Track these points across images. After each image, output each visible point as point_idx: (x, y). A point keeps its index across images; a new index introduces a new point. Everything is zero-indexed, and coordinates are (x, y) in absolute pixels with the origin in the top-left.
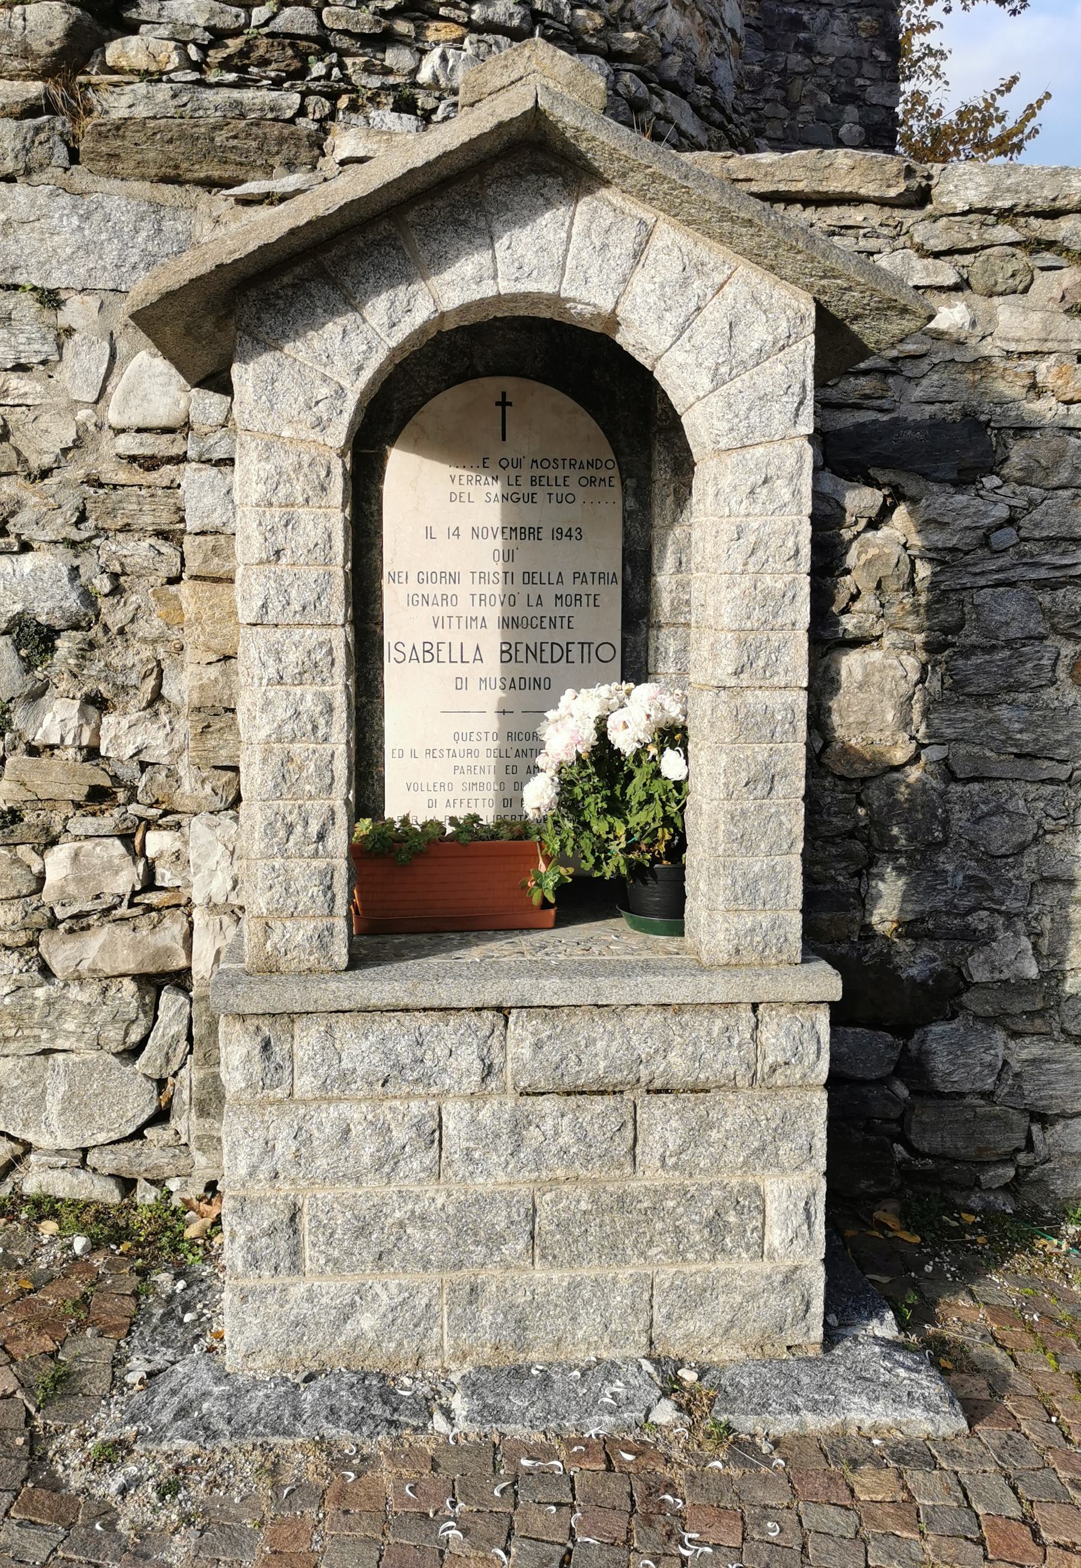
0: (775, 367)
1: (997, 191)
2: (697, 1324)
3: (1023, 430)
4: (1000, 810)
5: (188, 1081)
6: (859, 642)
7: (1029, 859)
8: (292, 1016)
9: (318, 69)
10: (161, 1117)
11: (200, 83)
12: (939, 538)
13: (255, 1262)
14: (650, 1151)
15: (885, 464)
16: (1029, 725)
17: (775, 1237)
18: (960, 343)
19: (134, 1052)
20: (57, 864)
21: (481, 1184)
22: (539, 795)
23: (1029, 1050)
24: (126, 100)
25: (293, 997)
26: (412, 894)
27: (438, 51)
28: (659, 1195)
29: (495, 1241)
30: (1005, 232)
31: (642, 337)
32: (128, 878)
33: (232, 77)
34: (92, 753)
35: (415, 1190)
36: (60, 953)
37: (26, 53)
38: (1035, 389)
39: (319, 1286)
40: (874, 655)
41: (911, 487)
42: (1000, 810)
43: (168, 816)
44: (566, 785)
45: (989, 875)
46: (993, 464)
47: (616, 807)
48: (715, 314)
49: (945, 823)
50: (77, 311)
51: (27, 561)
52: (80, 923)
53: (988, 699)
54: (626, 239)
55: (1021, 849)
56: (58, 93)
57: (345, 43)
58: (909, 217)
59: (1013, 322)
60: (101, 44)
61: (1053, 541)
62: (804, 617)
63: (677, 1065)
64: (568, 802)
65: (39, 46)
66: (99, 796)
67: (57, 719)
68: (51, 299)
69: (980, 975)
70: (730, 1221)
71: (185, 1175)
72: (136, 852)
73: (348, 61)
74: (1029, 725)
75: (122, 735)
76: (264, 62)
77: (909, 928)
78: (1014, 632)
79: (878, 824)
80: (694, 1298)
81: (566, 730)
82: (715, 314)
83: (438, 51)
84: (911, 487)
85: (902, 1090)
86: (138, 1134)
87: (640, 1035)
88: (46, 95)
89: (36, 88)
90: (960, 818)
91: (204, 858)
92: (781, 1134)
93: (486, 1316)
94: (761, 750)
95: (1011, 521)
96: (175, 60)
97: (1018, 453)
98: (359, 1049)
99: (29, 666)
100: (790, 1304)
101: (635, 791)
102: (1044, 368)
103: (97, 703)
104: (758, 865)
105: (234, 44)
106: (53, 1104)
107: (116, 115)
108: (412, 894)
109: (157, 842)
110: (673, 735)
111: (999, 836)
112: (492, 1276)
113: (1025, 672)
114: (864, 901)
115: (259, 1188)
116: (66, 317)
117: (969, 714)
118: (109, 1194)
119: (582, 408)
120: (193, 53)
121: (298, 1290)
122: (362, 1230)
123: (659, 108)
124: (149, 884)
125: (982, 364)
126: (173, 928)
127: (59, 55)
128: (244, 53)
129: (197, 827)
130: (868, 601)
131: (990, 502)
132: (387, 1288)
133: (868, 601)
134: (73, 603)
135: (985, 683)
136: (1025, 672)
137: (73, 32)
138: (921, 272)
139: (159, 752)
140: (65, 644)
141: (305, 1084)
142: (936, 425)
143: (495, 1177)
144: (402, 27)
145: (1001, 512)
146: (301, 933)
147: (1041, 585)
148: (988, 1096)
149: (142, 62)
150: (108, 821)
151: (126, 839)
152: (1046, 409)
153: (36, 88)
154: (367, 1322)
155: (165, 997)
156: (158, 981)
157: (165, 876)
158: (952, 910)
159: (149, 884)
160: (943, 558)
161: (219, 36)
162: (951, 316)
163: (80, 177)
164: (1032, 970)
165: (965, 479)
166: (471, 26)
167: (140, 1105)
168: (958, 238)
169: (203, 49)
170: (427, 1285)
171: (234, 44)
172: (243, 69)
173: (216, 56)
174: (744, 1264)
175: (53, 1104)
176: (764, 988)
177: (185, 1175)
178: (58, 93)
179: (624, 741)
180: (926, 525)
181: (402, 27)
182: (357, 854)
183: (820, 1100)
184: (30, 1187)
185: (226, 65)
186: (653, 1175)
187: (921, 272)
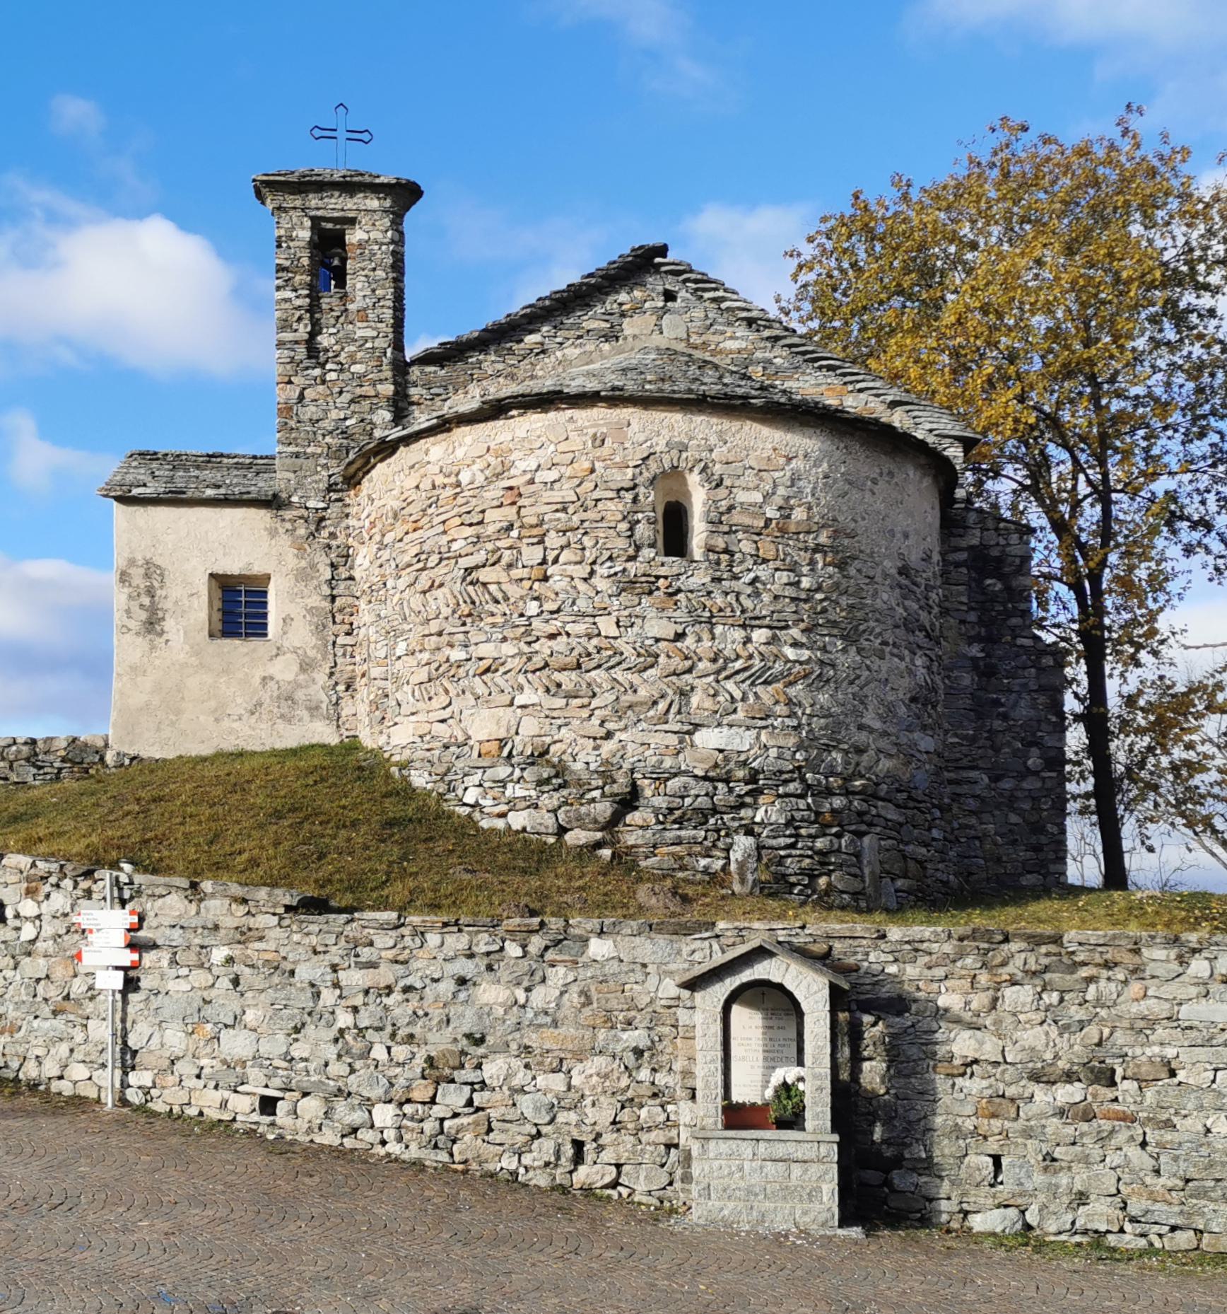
0: (819, 995)
1: (905, 936)
2: (807, 1219)
3: (915, 1001)
4: (913, 1108)
5: (679, 1173)
6: (870, 1059)
7: (922, 1123)
8: (709, 1139)
9: (712, 821)
10: (671, 1184)
11: (664, 829)
12: (891, 1030)
13: (700, 1196)
14: (793, 1176)
15: (875, 1009)
16: (921, 1084)
17: (825, 1199)
18: (896, 976)
19: (663, 1166)
20: (644, 1113)
21: (753, 1181)
22: (769, 1093)
23: (924, 1179)
24: (634, 837)
25: (709, 1134)
26: (738, 1117)
27: (763, 809)
28: (796, 1187)
29: (756, 1195)
30: (907, 947)
31: (790, 986)
32: (662, 1117)
33: (677, 826)
34: (653, 1083)
35: (736, 1181)
36: (644, 1137)
37: (596, 821)
38: (918, 989)
39: (714, 1203)
40: (874, 1063)
41: (883, 1016)
42: (913, 1108)
43: (673, 1101)
44: (776, 1091)
45: (910, 1125)
46: (908, 1010)
47: (789, 1097)
48: (805, 983)
49: (896, 1111)
50: (650, 969)
51: (637, 1032)
52: (649, 1129)
53: (908, 1076)
54: (784, 966)
55: (920, 1120)
56: (608, 837)
57: (724, 809)
58: (880, 942)
59: (911, 971)
60: (624, 815)
61: (926, 1032)
62: (829, 1051)
63: (800, 1156)
64: (777, 1095)
65: (601, 819)
66: (655, 1095)
67: (644, 1074)
68: (644, 966)
69: (907, 1156)
70: (814, 1194)
71: (678, 1199)
72: (665, 1111)
73: (725, 817)
74: (921, 1084)
75: (662, 1079)
76: (689, 820)
77: (884, 1141)
78: (915, 1057)
79: (876, 1111)
80: (805, 1213)
81: (778, 1076)
82: (805, 983)
83: (763, 809)
84: (883, 1016)
85: (886, 1190)
86: (664, 1188)
87: (791, 1148)
88: (603, 837)
89: (599, 835)
90: (901, 1111)
91: (684, 1112)
92: (825, 1173)
93: (755, 1214)
94: (819, 1083)
95: (913, 1026)
96: (654, 821)
97: (914, 1007)
98: (724, 1147)
99: (637, 1059)
100: (829, 1215)
101: (793, 1093)
102: (921, 984)
103: (654, 1070)
104: (819, 1109)
105: (678, 813)
106: (642, 1178)
107: (630, 843)
108: (738, 1117)
109: (670, 1108)
110: (801, 1079)
111: (913, 1116)
112: (756, 1204)
113: (919, 1069)
114: (872, 1133)
115: (701, 1179)
116: (648, 970)
117: (902, 1081)
118: (656, 1202)
119: (777, 1002)
120: (661, 817)
121: (710, 1203)
122: (725, 1190)
123: (874, 812)
124: (668, 1120)
125: (901, 982)
126: (674, 1132)
127: (608, 822)
128: (681, 817)
129: (682, 1103)
130: (871, 1048)
131: (908, 1019)
132: (731, 1205)
133: (871, 1048)
134: (649, 1043)
135: (906, 1072)
136: (919, 1069)
137: (613, 814)
138: (883, 957)
139: (671, 1084)
140: (646, 1054)
141: (712, 1155)
142: (890, 999)
143: (755, 1179)
144: (748, 800)
145: (909, 1023)
146: (711, 1120)
147: (922, 1044)
148: (913, 1193)
149: (640, 823)
150: (658, 1101)
151: (662, 1106)
152: (921, 995)
153: (599, 835)
154: (726, 1212)
155: (672, 1150)
156: (669, 1146)
157: (672, 1117)
158: (898, 1136)
159: (668, 1120)
160: (892, 1036)
161: (671, 810)
162: (892, 969)
163: (653, 935)
164: (924, 1155)
165: (899, 1014)
166: (779, 796)
167: (665, 1180)
168: (893, 948)
169: (665, 816)
170: (741, 1204)
171: (678, 813)
172: (681, 823)
173: (671, 818)
174: (818, 1207)
175: (642, 1178)
176: (820, 1138)
177: (678, 1199)
178: (608, 837)
179: (789, 1081)
180: (888, 1026)
181: (748, 800)
182: (724, 1107)
183: (836, 1166)
184: (636, 1199)
185: (674, 822)
186: (794, 1182)
187: (883, 957)
